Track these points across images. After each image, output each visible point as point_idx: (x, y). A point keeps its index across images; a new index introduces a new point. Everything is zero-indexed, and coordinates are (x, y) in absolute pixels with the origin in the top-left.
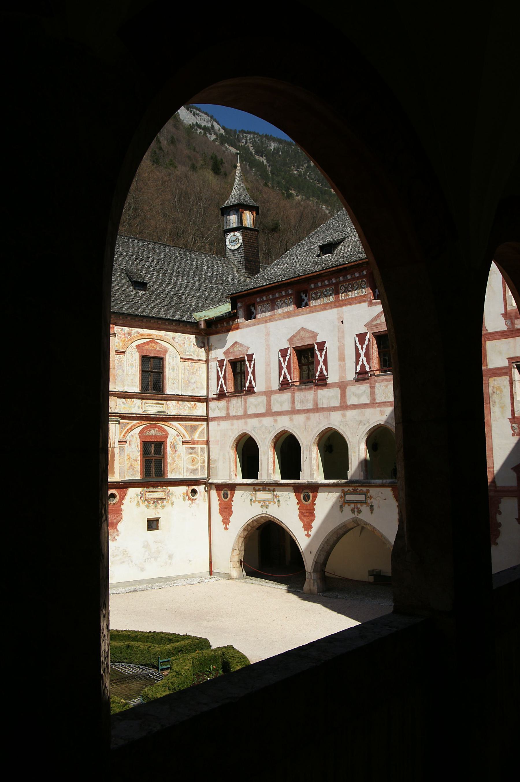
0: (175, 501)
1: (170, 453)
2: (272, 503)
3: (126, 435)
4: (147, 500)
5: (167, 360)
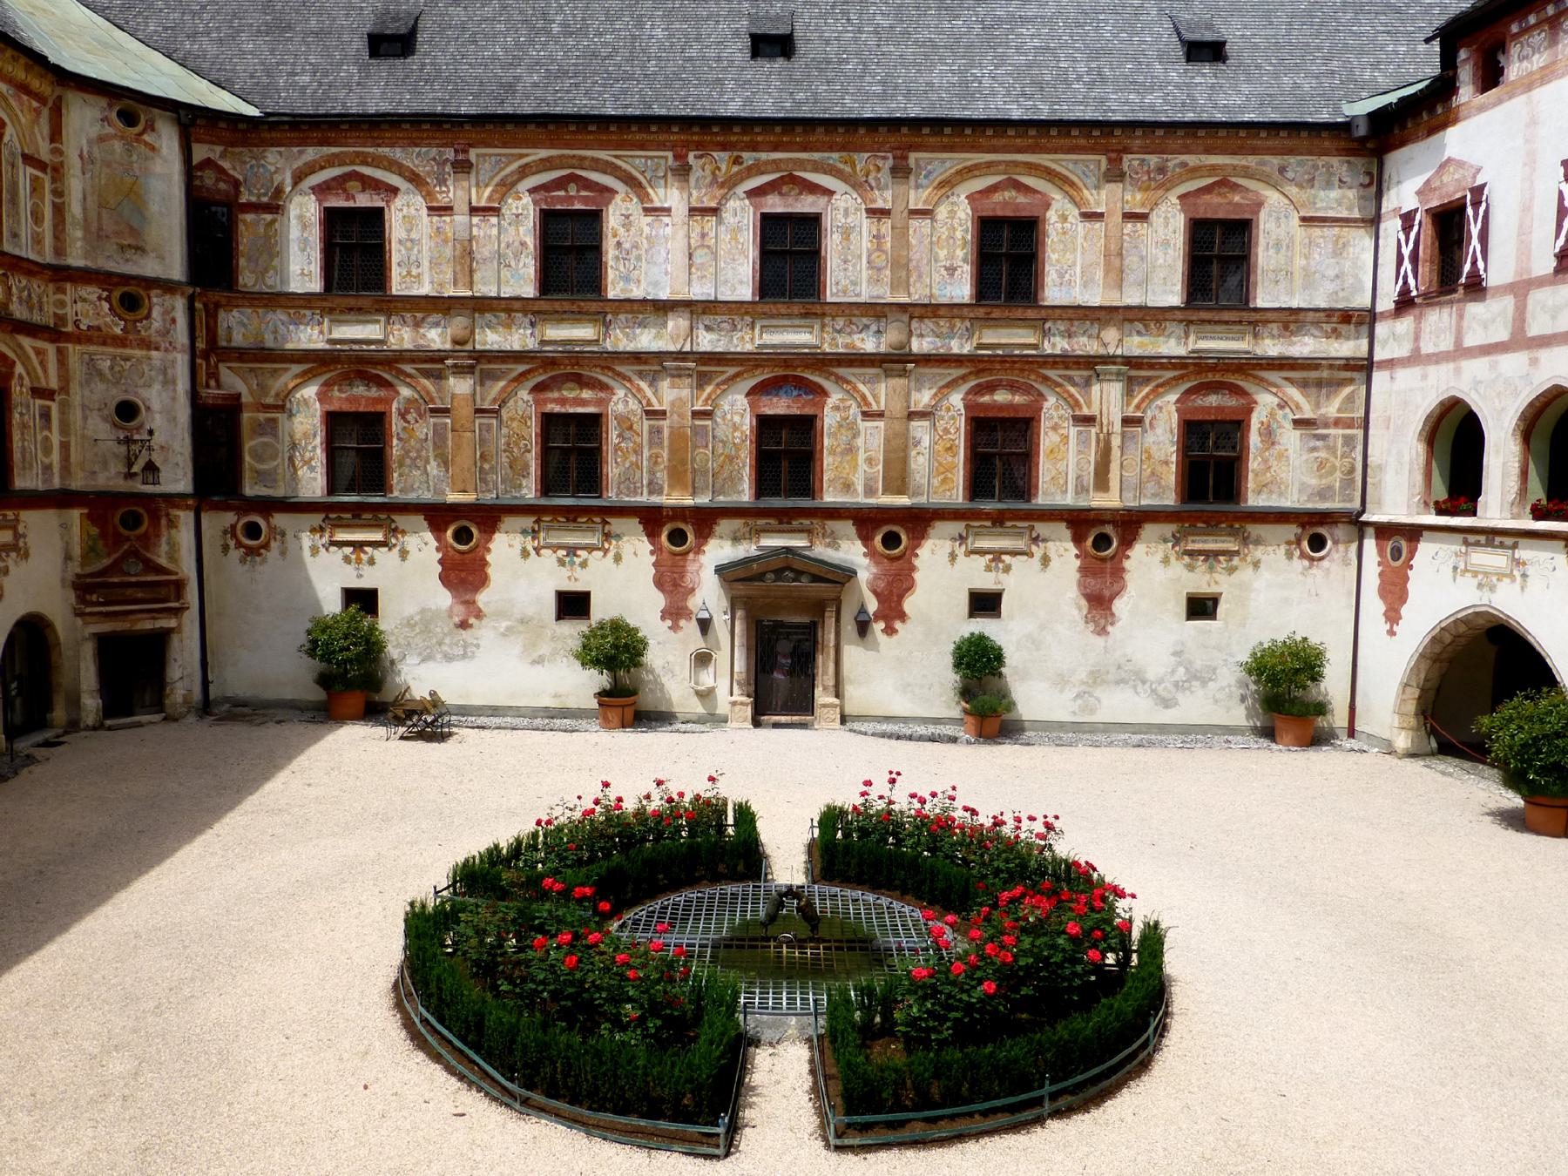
0: (1264, 558)
1: (1257, 449)
2: (1506, 580)
3: (1144, 405)
4: (1192, 554)
5: (1261, 227)
